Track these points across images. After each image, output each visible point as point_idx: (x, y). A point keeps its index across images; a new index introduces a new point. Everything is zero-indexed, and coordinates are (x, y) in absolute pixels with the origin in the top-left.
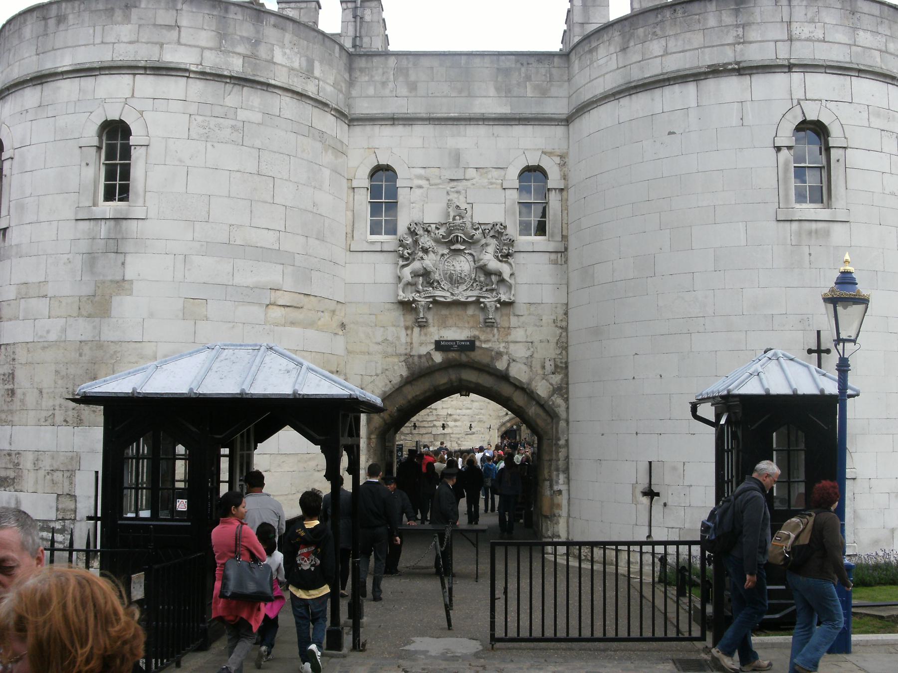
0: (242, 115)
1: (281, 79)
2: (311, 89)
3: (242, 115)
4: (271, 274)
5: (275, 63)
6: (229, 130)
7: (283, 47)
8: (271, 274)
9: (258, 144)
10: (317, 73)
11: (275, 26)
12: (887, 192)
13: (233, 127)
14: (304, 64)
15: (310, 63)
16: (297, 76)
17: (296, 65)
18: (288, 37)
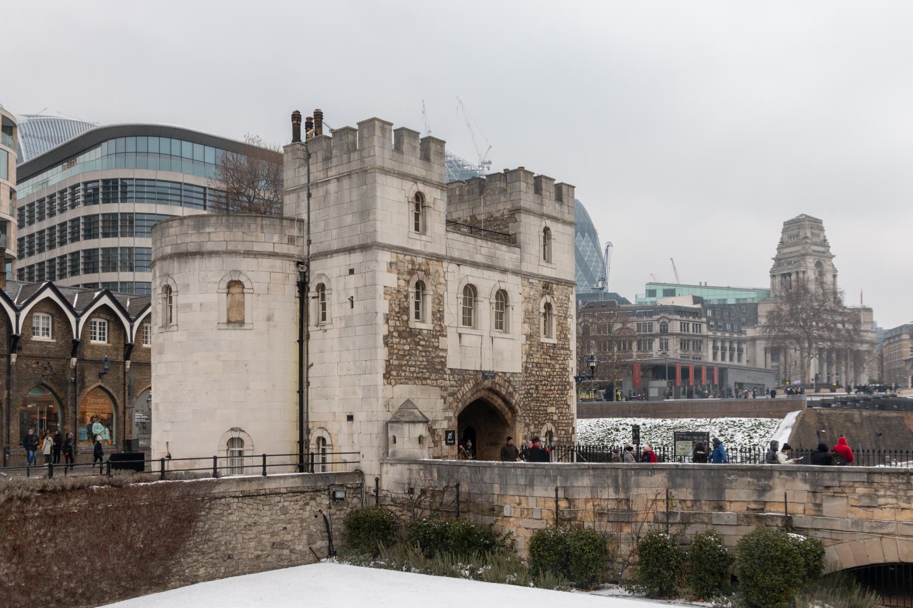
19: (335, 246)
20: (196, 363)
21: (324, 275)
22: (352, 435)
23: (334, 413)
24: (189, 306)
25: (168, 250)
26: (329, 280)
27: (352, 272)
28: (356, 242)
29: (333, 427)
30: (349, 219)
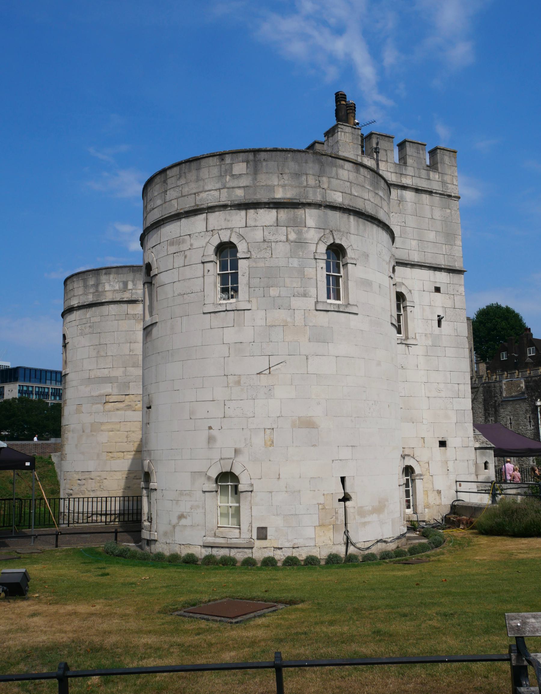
0: (93, 320)
1: (109, 297)
2: (126, 296)
3: (93, 320)
4: (107, 389)
5: (106, 291)
6: (88, 328)
7: (109, 282)
8: (107, 389)
9: (99, 331)
10: (130, 286)
11: (106, 274)
12: (176, 294)
13: (89, 326)
14: (121, 285)
15: (125, 284)
16: (118, 293)
17: (117, 287)
18: (112, 276)
19: (415, 258)
20: (379, 364)
21: (403, 284)
22: (446, 462)
23: (423, 438)
24: (366, 284)
25: (338, 198)
26: (410, 291)
27: (437, 290)
28: (442, 262)
29: (423, 454)
30: (431, 236)
